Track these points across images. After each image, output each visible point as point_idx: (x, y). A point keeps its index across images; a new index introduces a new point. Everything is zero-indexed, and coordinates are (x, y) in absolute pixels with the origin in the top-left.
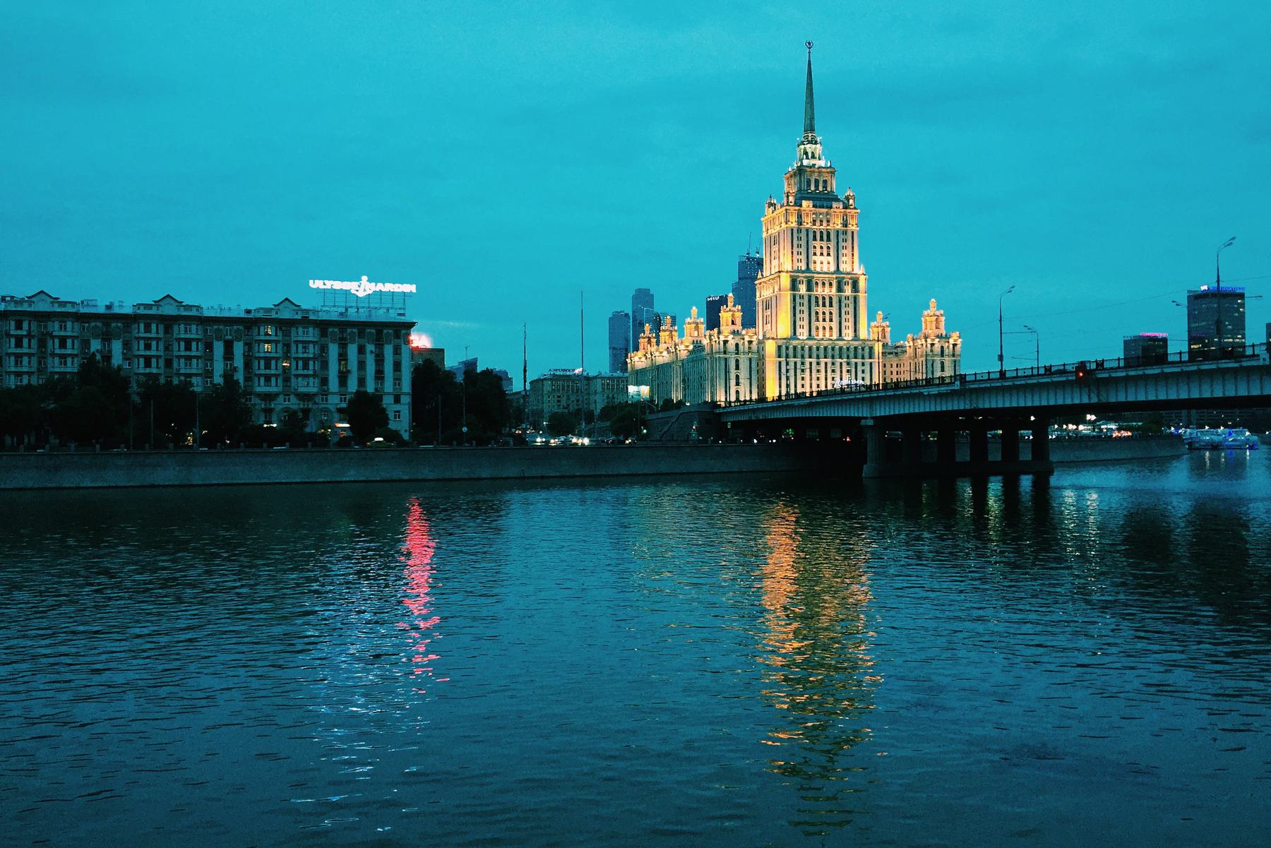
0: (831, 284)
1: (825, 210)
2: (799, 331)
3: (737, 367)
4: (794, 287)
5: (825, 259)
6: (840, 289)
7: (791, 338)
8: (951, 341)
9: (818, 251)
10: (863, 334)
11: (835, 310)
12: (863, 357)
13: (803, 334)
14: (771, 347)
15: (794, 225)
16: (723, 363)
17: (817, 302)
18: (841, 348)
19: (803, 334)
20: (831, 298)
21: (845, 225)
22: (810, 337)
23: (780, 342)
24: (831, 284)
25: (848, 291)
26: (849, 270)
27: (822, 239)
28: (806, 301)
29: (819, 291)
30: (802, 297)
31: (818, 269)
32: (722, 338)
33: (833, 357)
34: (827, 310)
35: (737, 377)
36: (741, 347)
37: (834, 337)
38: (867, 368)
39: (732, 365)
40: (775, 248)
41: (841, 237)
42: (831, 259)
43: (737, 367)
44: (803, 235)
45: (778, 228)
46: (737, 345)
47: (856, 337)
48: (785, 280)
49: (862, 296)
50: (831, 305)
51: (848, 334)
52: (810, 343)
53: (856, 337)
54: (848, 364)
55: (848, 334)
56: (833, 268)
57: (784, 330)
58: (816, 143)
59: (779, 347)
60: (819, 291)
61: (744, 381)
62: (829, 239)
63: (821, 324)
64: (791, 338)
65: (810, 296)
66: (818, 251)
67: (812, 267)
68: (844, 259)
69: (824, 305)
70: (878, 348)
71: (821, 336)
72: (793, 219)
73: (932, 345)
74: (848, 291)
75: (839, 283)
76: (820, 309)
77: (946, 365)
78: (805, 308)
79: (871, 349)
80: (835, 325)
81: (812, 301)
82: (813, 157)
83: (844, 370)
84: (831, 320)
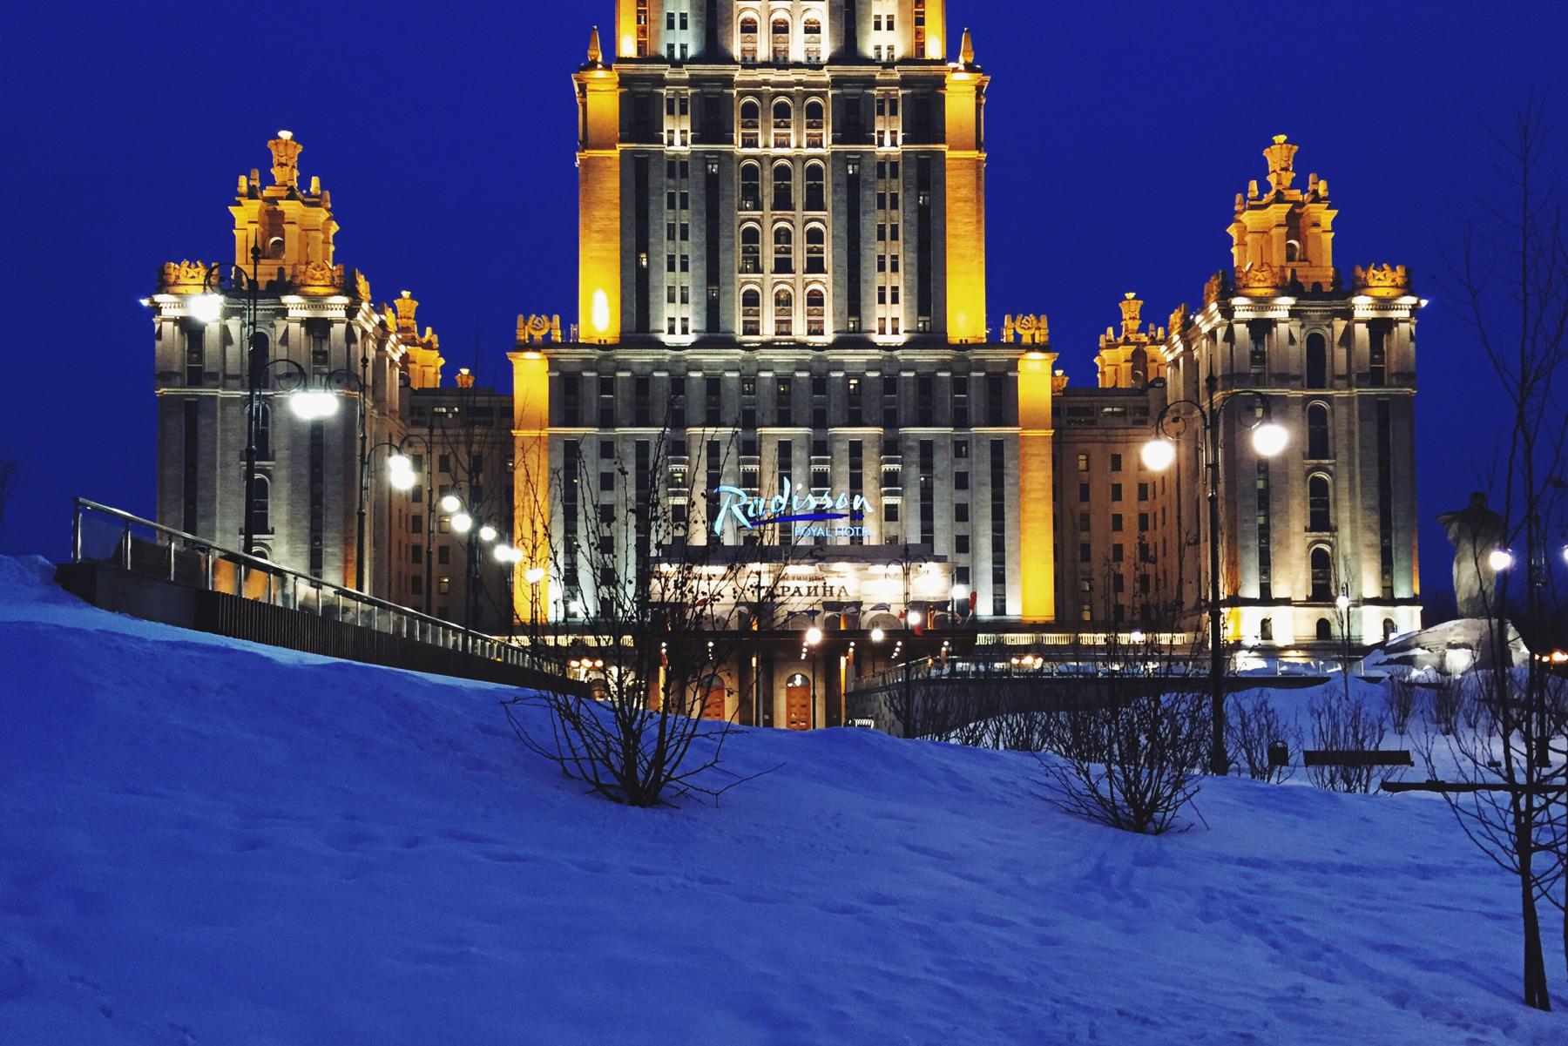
8: (1363, 306)
10: (966, 314)
11: (825, 220)
12: (961, 421)
13: (677, 320)
14: (531, 378)
17: (752, 194)
22: (714, 335)
23: (569, 356)
24: (814, 113)
25: (889, 139)
28: (693, 188)
30: (677, 167)
33: (819, 421)
34: (799, 220)
36: (276, 351)
37: (828, 337)
38: (981, 468)
47: (931, 334)
49: (961, 162)
50: (815, 202)
51: (890, 321)
53: (931, 334)
54: (890, 447)
61: (279, 512)
63: (768, 283)
69: (783, 201)
70: (1036, 379)
73: (1260, 328)
74: (889, 139)
76: (768, 221)
77: (1339, 423)
79: (1001, 386)
80: (825, 283)
83: (871, 472)
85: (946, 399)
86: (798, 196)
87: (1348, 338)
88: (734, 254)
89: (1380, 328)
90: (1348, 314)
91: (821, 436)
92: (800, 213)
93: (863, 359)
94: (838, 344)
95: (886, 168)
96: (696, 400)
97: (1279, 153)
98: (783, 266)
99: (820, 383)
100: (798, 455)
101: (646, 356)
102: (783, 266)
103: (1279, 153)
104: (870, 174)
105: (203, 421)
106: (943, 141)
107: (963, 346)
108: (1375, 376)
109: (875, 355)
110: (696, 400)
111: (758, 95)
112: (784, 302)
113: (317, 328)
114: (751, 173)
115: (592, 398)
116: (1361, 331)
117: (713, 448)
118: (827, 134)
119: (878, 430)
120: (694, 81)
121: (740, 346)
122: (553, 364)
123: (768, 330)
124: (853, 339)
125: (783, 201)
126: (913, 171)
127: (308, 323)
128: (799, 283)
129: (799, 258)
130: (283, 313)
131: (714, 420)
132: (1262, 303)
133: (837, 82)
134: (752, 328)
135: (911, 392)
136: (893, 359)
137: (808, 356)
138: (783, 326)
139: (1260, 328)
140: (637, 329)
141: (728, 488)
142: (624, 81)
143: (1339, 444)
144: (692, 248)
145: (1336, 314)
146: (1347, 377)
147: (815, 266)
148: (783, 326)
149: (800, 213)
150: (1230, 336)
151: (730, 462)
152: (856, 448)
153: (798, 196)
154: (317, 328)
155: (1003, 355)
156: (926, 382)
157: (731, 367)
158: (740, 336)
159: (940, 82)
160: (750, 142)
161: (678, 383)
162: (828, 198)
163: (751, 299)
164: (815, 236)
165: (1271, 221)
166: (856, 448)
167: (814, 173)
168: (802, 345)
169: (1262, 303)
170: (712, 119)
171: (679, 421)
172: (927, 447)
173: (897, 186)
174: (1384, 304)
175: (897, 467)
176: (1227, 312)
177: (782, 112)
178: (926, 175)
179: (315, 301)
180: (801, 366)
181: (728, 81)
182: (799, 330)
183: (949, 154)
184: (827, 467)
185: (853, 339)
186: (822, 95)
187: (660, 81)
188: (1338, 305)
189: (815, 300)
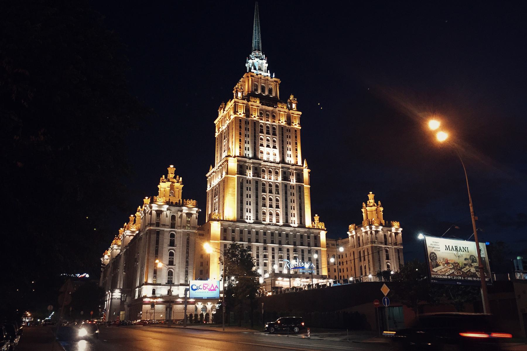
0: (277, 173)
1: (271, 108)
2: (246, 214)
3: (172, 244)
4: (241, 169)
5: (271, 150)
6: (286, 178)
7: (238, 221)
8: (393, 230)
9: (265, 143)
11: (280, 197)
12: (309, 245)
13: (250, 217)
15: (242, 116)
16: (154, 237)
18: (287, 235)
19: (250, 217)
20: (277, 186)
21: (289, 121)
22: (257, 221)
23: (227, 223)
24: (277, 173)
26: (293, 162)
27: (268, 133)
29: (266, 178)
30: (249, 182)
31: (265, 158)
32: (155, 207)
35: (171, 254)
36: (178, 220)
37: (281, 223)
39: (167, 240)
40: (225, 142)
41: (286, 134)
42: (277, 151)
43: (172, 244)
44: (250, 127)
45: (228, 122)
46: (173, 217)
47: (302, 224)
48: (233, 165)
51: (295, 221)
52: (258, 226)
53: (302, 224)
54: (295, 250)
55: (295, 221)
56: (278, 159)
57: (230, 211)
58: (262, 59)
59: (224, 230)
60: (266, 178)
61: (177, 260)
62: (274, 134)
63: (267, 210)
64: (238, 221)
65: (257, 182)
66: (265, 143)
67: (260, 156)
68: (289, 152)
69: (271, 192)
71: (268, 221)
72: (241, 113)
73: (377, 232)
74: (293, 181)
75: (284, 173)
76: (267, 195)
78: (252, 193)
79: (317, 238)
80: (280, 211)
81: (259, 187)
82: (260, 69)
83: (292, 255)
84: (277, 207)
85: (306, 240)
86: (274, 191)
87: (391, 235)
88: (260, 203)
89: (396, 234)
90: (391, 231)
91: (265, 245)
92: (274, 195)
93: (289, 229)
94: (284, 225)
95: (292, 187)
96: (253, 236)
97: (371, 196)
98: (271, 206)
99: (280, 235)
100: (276, 251)
101: (243, 225)
102: (271, 206)
103: (371, 196)
104: (289, 188)
105: (160, 236)
106: (303, 183)
107: (309, 228)
108: (396, 244)
109: (292, 229)
110: (253, 236)
111: (265, 168)
112: (271, 214)
113: (189, 215)
114: (264, 185)
115: (230, 234)
116: (393, 234)
117: (258, 248)
118: (280, 179)
119: (293, 246)
120: (253, 163)
121: (263, 224)
122: (222, 225)
123: (268, 221)
124: (287, 224)
125: (271, 192)
126: (298, 188)
127: (187, 214)
128: (273, 210)
129: (274, 205)
130: (181, 211)
131: (257, 241)
132: (377, 227)
133: (282, 167)
134: (265, 221)
135: (299, 237)
136: (295, 230)
137: (278, 228)
138: (271, 220)
139: (377, 232)
140: (240, 219)
141: (276, 259)
142: (238, 161)
143: (391, 257)
144: (252, 200)
145: (388, 230)
146: (391, 243)
147: (277, 207)
148: (271, 220)
149: (274, 195)
150: (371, 233)
151: (261, 253)
152: (288, 250)
153: (274, 191)
154: (189, 215)
155: (317, 231)
156: (302, 236)
157: (261, 229)
158: (263, 222)
159: (302, 170)
160: (264, 178)
161: (249, 232)
162: (280, 192)
163: (264, 213)
164: (277, 200)
165: (371, 209)
166: (288, 250)
167: (277, 186)
168: (276, 225)
169: (377, 227)
170: (257, 172)
171: (249, 241)
172: (303, 251)
173: (294, 191)
174: (397, 229)
175: (297, 255)
176: (371, 228)
177: (270, 172)
178: (300, 189)
179: (190, 209)
180: (276, 230)
181: (260, 164)
182: (274, 221)
183: (305, 186)
184: (282, 254)
185: (287, 224)
186: (279, 170)
187: (246, 162)
188: (389, 229)
189: (277, 215)
